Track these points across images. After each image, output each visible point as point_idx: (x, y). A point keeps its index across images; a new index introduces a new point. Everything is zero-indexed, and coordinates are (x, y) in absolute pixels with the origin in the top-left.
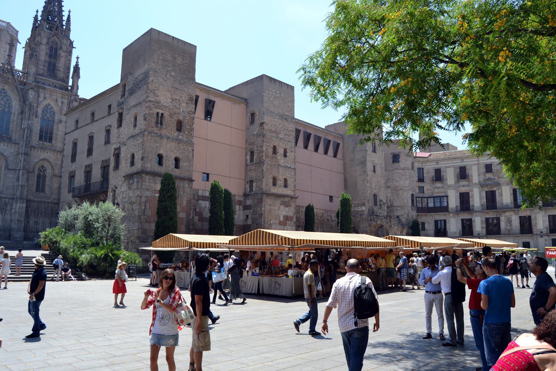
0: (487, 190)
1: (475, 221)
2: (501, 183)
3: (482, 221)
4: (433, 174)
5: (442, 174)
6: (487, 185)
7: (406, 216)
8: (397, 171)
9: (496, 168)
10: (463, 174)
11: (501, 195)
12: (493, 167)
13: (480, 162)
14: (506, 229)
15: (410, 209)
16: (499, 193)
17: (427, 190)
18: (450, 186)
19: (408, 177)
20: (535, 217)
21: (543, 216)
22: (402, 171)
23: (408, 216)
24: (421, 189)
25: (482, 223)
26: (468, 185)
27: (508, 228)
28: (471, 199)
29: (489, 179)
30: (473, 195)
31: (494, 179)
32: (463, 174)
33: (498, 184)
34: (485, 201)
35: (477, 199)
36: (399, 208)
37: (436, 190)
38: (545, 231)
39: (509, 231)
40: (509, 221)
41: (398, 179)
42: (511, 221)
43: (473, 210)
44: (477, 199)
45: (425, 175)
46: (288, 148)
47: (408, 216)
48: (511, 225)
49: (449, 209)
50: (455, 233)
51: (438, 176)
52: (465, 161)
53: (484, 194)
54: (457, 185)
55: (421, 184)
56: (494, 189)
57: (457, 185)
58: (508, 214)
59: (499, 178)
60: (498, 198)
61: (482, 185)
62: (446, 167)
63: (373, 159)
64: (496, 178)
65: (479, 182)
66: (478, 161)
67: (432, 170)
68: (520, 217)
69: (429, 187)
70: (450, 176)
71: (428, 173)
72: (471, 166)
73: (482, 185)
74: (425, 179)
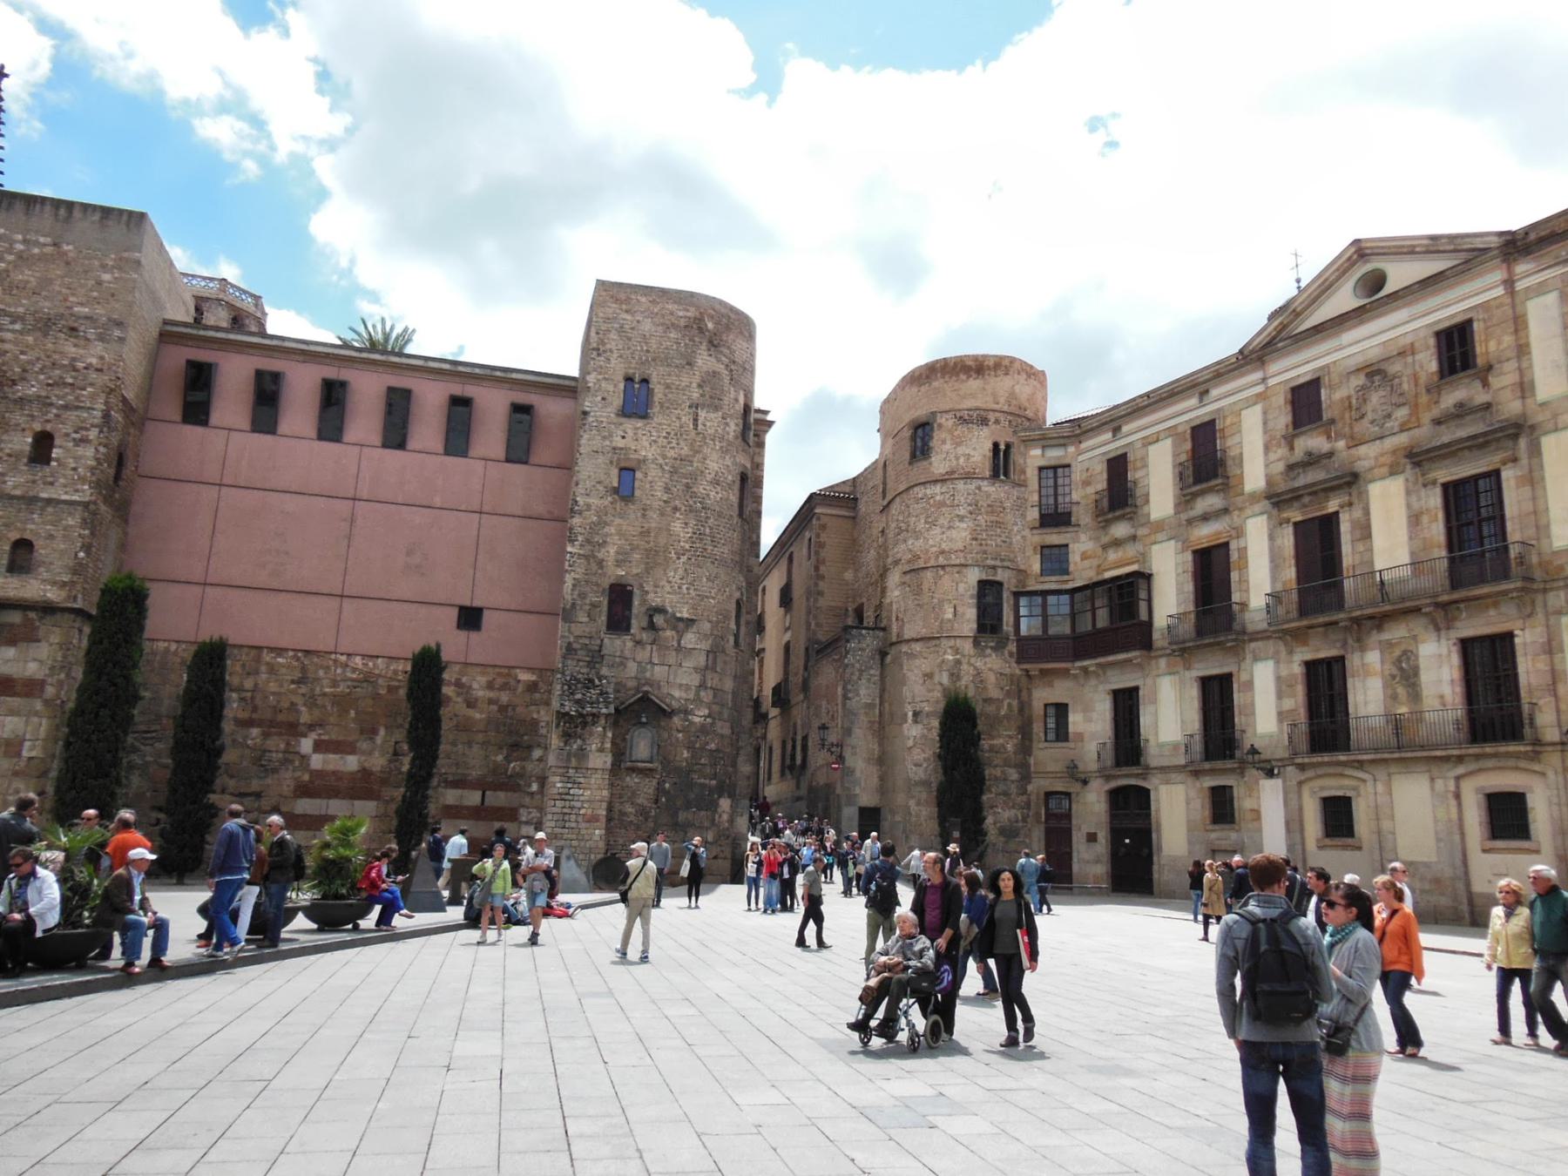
1: (1249, 685)
2: (1361, 466)
7: (945, 680)
8: (920, 492)
10: (1206, 461)
15: (967, 647)
16: (1355, 525)
17: (1084, 556)
18: (1159, 526)
19: (962, 512)
22: (937, 489)
23: (955, 676)
24: (1055, 559)
26: (1226, 511)
27: (1403, 710)
28: (1234, 576)
30: (1243, 551)
31: (1330, 454)
32: (1206, 461)
33: (1351, 481)
34: (1291, 573)
36: (917, 647)
37: (1113, 556)
40: (1406, 674)
41: (921, 525)
42: (1415, 671)
43: (1244, 632)
46: (61, 430)
47: (955, 676)
48: (1415, 695)
50: (1176, 746)
51: (1120, 492)
52: (1215, 393)
53: (1287, 539)
54: (1184, 516)
55: (1054, 538)
56: (1332, 506)
57: (1184, 516)
58: (1397, 632)
59: (1354, 442)
60: (1349, 553)
61: (1277, 499)
63: (620, 443)
66: (1264, 380)
68: (1466, 645)
71: (1086, 483)
73: (1277, 499)
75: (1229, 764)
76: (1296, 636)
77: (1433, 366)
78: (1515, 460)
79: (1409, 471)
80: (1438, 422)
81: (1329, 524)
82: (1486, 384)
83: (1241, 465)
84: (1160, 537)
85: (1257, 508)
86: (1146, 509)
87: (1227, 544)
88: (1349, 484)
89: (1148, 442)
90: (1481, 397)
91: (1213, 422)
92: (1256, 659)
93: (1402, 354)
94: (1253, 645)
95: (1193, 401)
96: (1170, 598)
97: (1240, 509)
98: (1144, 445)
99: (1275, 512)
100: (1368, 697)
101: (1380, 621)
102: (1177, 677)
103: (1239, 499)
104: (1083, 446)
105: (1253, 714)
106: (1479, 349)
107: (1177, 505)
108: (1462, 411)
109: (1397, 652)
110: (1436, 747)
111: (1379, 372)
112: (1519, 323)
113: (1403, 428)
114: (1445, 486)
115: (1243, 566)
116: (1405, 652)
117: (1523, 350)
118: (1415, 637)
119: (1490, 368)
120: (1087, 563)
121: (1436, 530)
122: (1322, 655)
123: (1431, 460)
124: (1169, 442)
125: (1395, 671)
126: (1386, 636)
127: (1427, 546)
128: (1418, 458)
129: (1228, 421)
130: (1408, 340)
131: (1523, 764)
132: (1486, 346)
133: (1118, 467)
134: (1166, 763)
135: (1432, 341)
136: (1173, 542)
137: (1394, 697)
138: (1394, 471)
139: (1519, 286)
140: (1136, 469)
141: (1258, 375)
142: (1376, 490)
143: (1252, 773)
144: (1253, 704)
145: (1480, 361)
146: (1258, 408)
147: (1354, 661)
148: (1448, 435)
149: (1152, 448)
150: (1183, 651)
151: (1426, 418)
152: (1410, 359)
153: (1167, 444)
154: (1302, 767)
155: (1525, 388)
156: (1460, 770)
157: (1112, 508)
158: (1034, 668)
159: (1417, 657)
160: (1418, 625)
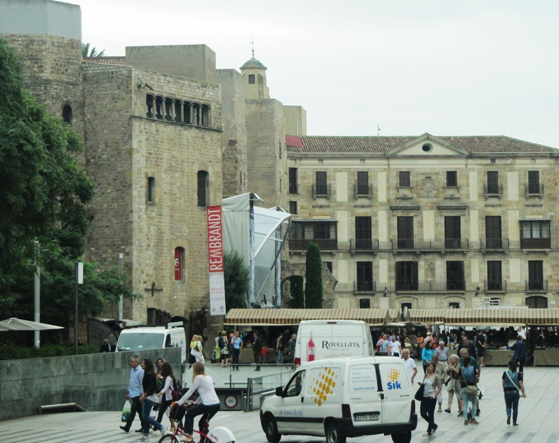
1: (378, 266)
2: (421, 204)
3: (389, 267)
4: (312, 180)
5: (328, 182)
9: (415, 179)
10: (363, 186)
11: (421, 225)
12: (411, 177)
13: (391, 167)
14: (426, 282)
16: (419, 222)
17: (302, 208)
18: (341, 204)
20: (470, 263)
21: (480, 263)
25: (390, 271)
26: (370, 206)
27: (429, 279)
28: (373, 229)
30: (377, 222)
31: (411, 198)
32: (363, 186)
33: (417, 208)
34: (396, 233)
35: (384, 232)
37: (317, 210)
38: (482, 286)
39: (430, 285)
40: (431, 269)
42: (434, 269)
44: (384, 232)
45: (299, 181)
48: (434, 275)
49: (338, 244)
50: (346, 285)
52: (367, 162)
53: (395, 222)
54: (353, 204)
55: (294, 198)
58: (430, 257)
59: (420, 196)
62: (336, 171)
64: (415, 196)
65: (389, 201)
67: (311, 174)
68: (448, 262)
69: (305, 204)
70: (342, 186)
71: (304, 178)
72: (377, 172)
74: (300, 189)
75: (371, 292)
76: (399, 254)
77: (445, 181)
78: (465, 215)
79: (436, 210)
80: (445, 198)
81: (409, 220)
82: (458, 191)
83: (377, 191)
84: (341, 208)
85: (383, 208)
86: (334, 196)
87: (370, 218)
88: (418, 209)
89: (336, 171)
90: (457, 195)
92: (381, 258)
94: (380, 254)
97: (376, 207)
98: (335, 171)
99: (391, 211)
101: (425, 253)
102: (347, 261)
103: (376, 203)
104: (303, 162)
105: (379, 276)
106: (458, 181)
107: (349, 198)
108: (452, 198)
109: (429, 263)
110: (437, 290)
111: (430, 178)
113: (435, 197)
114: (446, 217)
115: (377, 226)
116: (431, 263)
117: (468, 185)
118: (435, 259)
119: (460, 188)
120: (304, 210)
121: (443, 229)
122: (406, 260)
123: (444, 209)
124: (346, 173)
125: (428, 268)
126: (426, 257)
127: (440, 233)
128: (440, 208)
129: (373, 174)
130: (438, 170)
131: (461, 296)
132: (460, 181)
133: (321, 177)
134: (341, 290)
135: (445, 174)
136: (347, 211)
137: (427, 275)
138: (431, 208)
139: (468, 167)
140: (330, 179)
141: (385, 162)
143: (377, 295)
144: (379, 272)
145: (458, 185)
149: (338, 175)
150: (351, 253)
151: (442, 196)
152: (438, 176)
153: (346, 174)
154: (398, 294)
155: (468, 196)
156: (445, 296)
157: (318, 192)
158: (292, 251)
159: (435, 265)
160: (436, 257)
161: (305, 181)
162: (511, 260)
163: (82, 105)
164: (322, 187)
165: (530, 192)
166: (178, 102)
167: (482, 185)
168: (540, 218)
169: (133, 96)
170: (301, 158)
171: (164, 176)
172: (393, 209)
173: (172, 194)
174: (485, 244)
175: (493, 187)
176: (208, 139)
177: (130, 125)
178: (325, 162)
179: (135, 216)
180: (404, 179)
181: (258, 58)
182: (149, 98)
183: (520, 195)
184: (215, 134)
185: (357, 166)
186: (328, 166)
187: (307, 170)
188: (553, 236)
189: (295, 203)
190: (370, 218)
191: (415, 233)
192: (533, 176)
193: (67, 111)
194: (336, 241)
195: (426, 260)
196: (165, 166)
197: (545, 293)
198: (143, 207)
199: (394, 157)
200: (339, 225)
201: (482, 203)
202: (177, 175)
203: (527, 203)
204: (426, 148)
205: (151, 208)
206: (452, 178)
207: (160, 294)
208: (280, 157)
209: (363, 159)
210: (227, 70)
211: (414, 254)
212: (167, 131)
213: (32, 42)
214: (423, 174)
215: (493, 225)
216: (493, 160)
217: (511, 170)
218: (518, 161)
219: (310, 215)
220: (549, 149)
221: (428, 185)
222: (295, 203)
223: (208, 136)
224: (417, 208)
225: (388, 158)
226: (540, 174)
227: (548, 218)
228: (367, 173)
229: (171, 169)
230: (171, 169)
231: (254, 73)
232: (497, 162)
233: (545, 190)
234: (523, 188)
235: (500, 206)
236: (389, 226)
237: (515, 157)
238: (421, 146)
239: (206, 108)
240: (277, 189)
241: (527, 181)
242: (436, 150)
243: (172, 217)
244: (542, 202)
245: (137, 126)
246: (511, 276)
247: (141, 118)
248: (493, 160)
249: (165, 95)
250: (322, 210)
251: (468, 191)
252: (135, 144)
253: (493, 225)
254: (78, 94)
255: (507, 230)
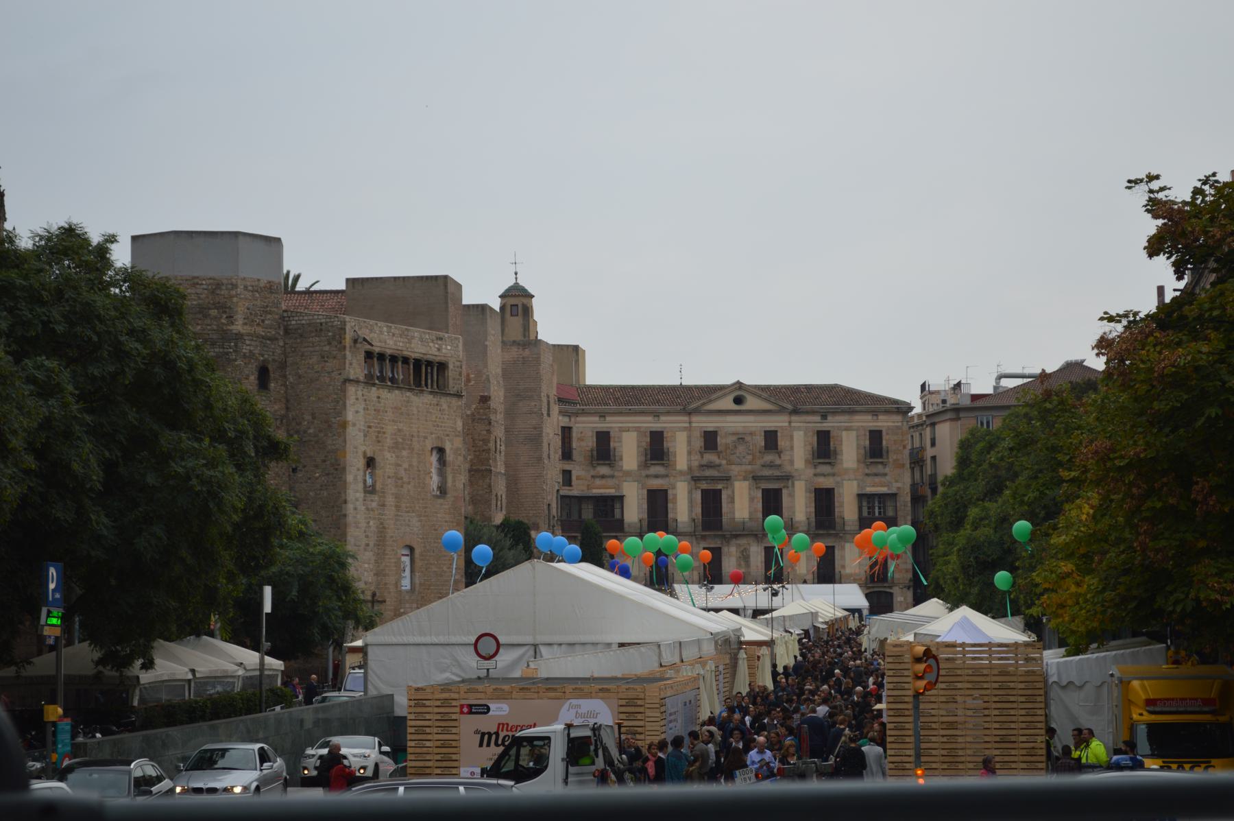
0: (705, 486)
2: (732, 474)
4: (591, 443)
5: (612, 444)
6: (706, 478)
10: (656, 449)
11: (732, 501)
17: (578, 478)
18: (628, 474)
26: (667, 476)
28: (670, 505)
29: (710, 466)
30: (675, 496)
31: (719, 465)
32: (656, 449)
33: (727, 479)
34: (699, 510)
37: (598, 482)
42: (748, 557)
45: (574, 445)
52: (663, 418)
53: (698, 496)
54: (644, 473)
56: (719, 487)
58: (743, 541)
59: (730, 463)
62: (622, 430)
65: (690, 468)
67: (590, 434)
69: (582, 473)
70: (629, 451)
71: (581, 439)
74: (576, 455)
76: (704, 538)
77: (763, 444)
87: (666, 491)
89: (622, 430)
90: (778, 462)
91: (662, 433)
93: (751, 434)
95: (650, 418)
96: (634, 510)
100: (730, 565)
101: (736, 536)
112: (792, 437)
114: (764, 490)
115: (675, 503)
117: (792, 448)
124: (635, 434)
132: (782, 443)
133: (603, 439)
137: (739, 565)
138: (745, 479)
141: (686, 418)
142: (737, 484)
146: (685, 434)
147: (725, 550)
148: (767, 472)
149: (624, 434)
151: (759, 462)
155: (792, 462)
161: (583, 444)
162: (847, 545)
163: (283, 366)
164: (604, 450)
165: (871, 457)
166: (406, 360)
167: (809, 448)
168: (884, 490)
169: (347, 353)
170: (576, 414)
171: (388, 455)
172: (696, 479)
173: (398, 478)
174: (813, 524)
175: (824, 449)
176: (445, 406)
177: (344, 391)
178: (608, 419)
179: (350, 506)
180: (710, 440)
181: (521, 283)
182: (369, 355)
183: (858, 461)
184: (454, 401)
185: (649, 423)
186: (612, 423)
187: (585, 428)
188: (899, 513)
189: (570, 472)
190: (666, 491)
191: (725, 510)
192: (876, 436)
193: (264, 374)
194: (622, 521)
195: (738, 546)
196: (389, 441)
197: (890, 587)
198: (360, 495)
199: (697, 411)
200: (626, 501)
201: (810, 472)
202: (405, 453)
203: (867, 471)
204: (738, 400)
205: (370, 497)
206: (771, 438)
207: (382, 607)
208: (549, 415)
209: (657, 415)
210: (477, 306)
211: (723, 536)
212: (391, 397)
213: (219, 285)
214: (733, 434)
215: (824, 500)
216: (824, 417)
217: (847, 429)
218: (857, 417)
219: (589, 487)
220: (896, 402)
221: (741, 448)
222: (570, 472)
223: (444, 401)
224: (727, 479)
225: (690, 414)
226: (884, 433)
227: (894, 491)
228: (662, 433)
229: (396, 447)
230: (396, 447)
231: (518, 302)
232: (829, 418)
233: (891, 455)
234: (862, 451)
235: (834, 475)
236: (691, 501)
237: (852, 412)
238: (731, 398)
239: (442, 366)
240: (545, 455)
241: (867, 442)
242: (752, 403)
243: (398, 507)
244: (887, 470)
245: (351, 390)
246: (847, 562)
247: (357, 382)
248: (824, 417)
249: (389, 352)
250: (603, 482)
251: (792, 456)
252: (350, 416)
253: (824, 500)
254: (278, 351)
255: (842, 506)
